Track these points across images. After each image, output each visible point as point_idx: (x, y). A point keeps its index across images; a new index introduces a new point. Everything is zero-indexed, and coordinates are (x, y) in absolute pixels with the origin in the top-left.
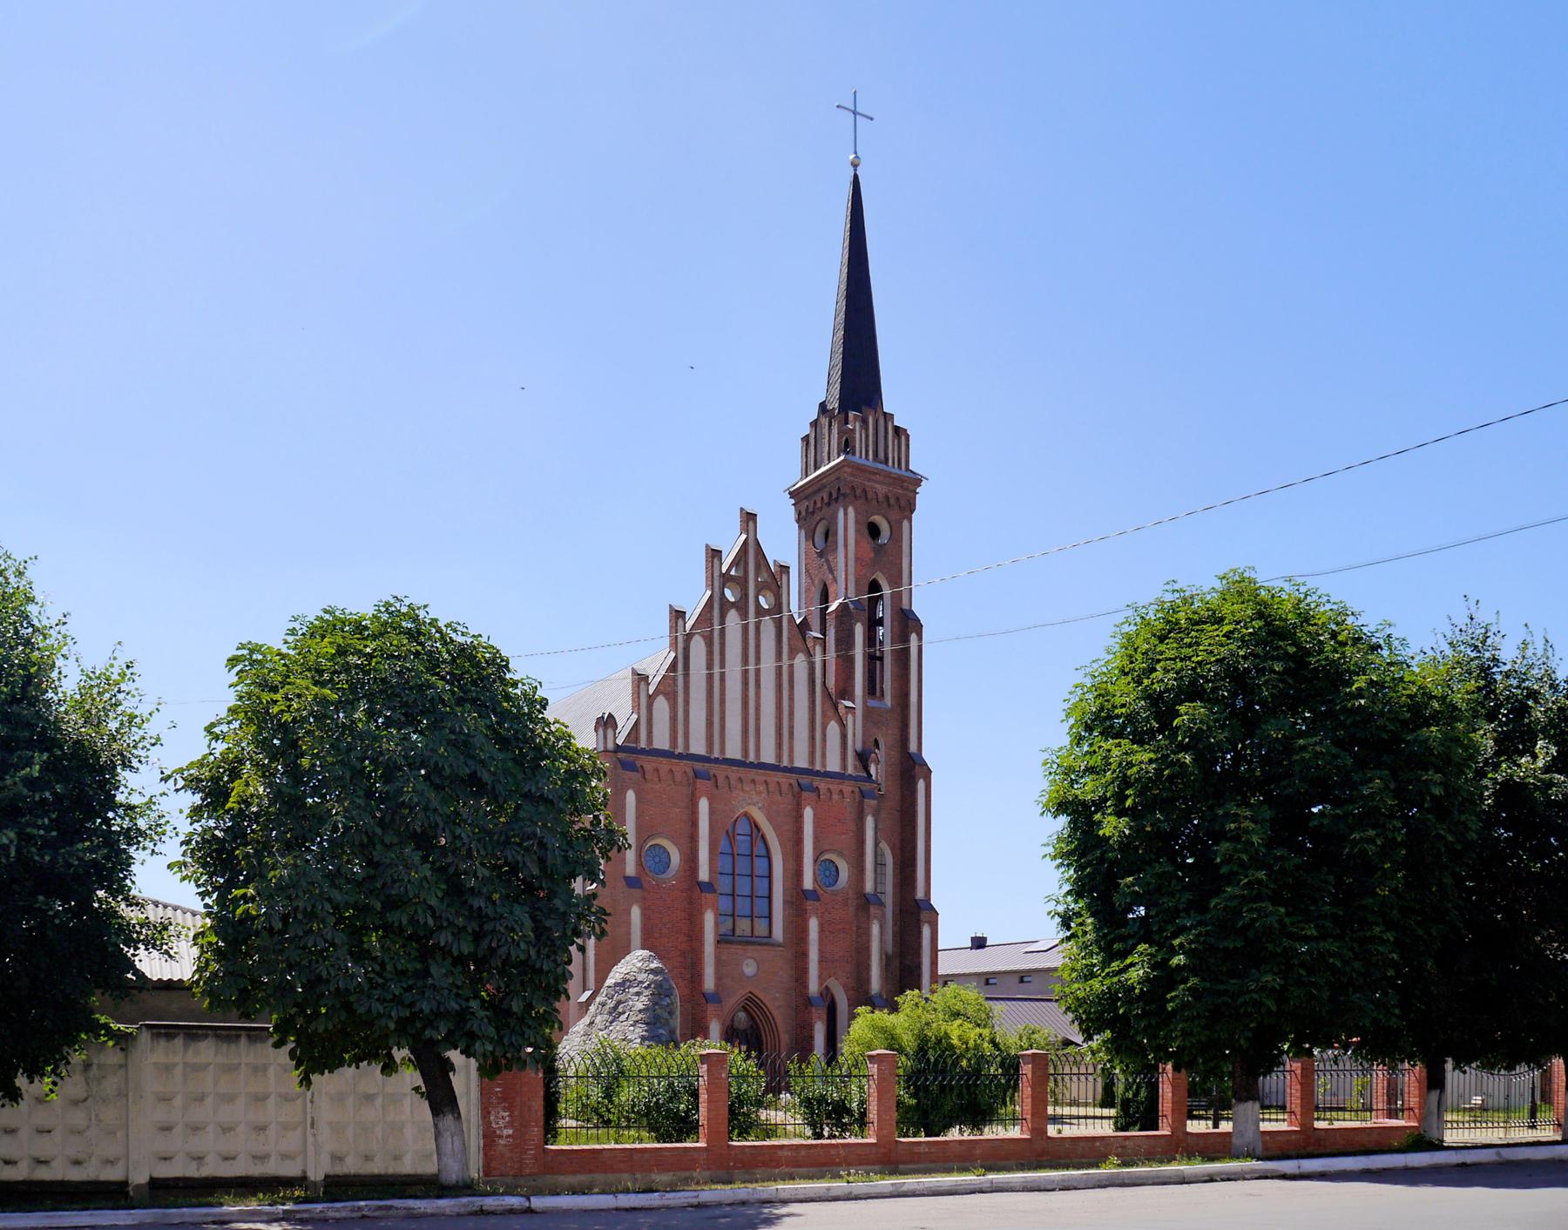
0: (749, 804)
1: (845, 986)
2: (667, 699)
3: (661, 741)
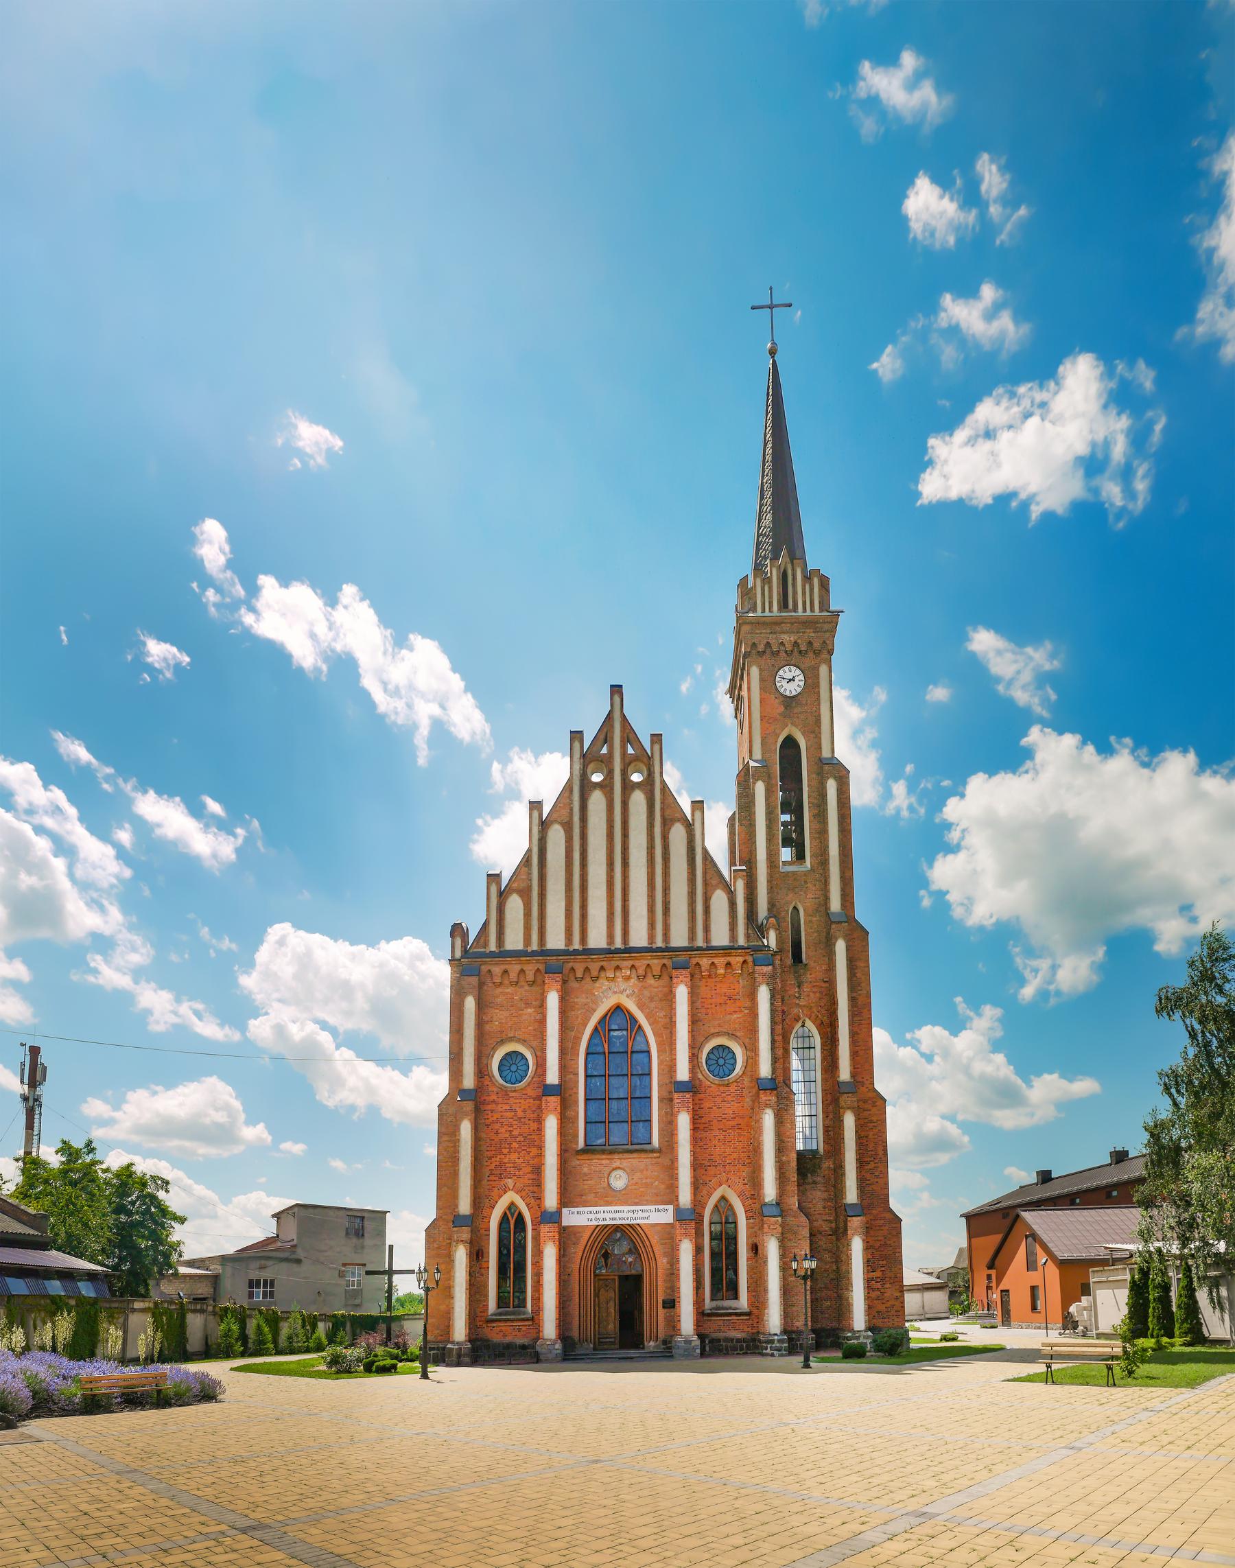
0: (615, 993)
2: (521, 896)
3: (514, 941)
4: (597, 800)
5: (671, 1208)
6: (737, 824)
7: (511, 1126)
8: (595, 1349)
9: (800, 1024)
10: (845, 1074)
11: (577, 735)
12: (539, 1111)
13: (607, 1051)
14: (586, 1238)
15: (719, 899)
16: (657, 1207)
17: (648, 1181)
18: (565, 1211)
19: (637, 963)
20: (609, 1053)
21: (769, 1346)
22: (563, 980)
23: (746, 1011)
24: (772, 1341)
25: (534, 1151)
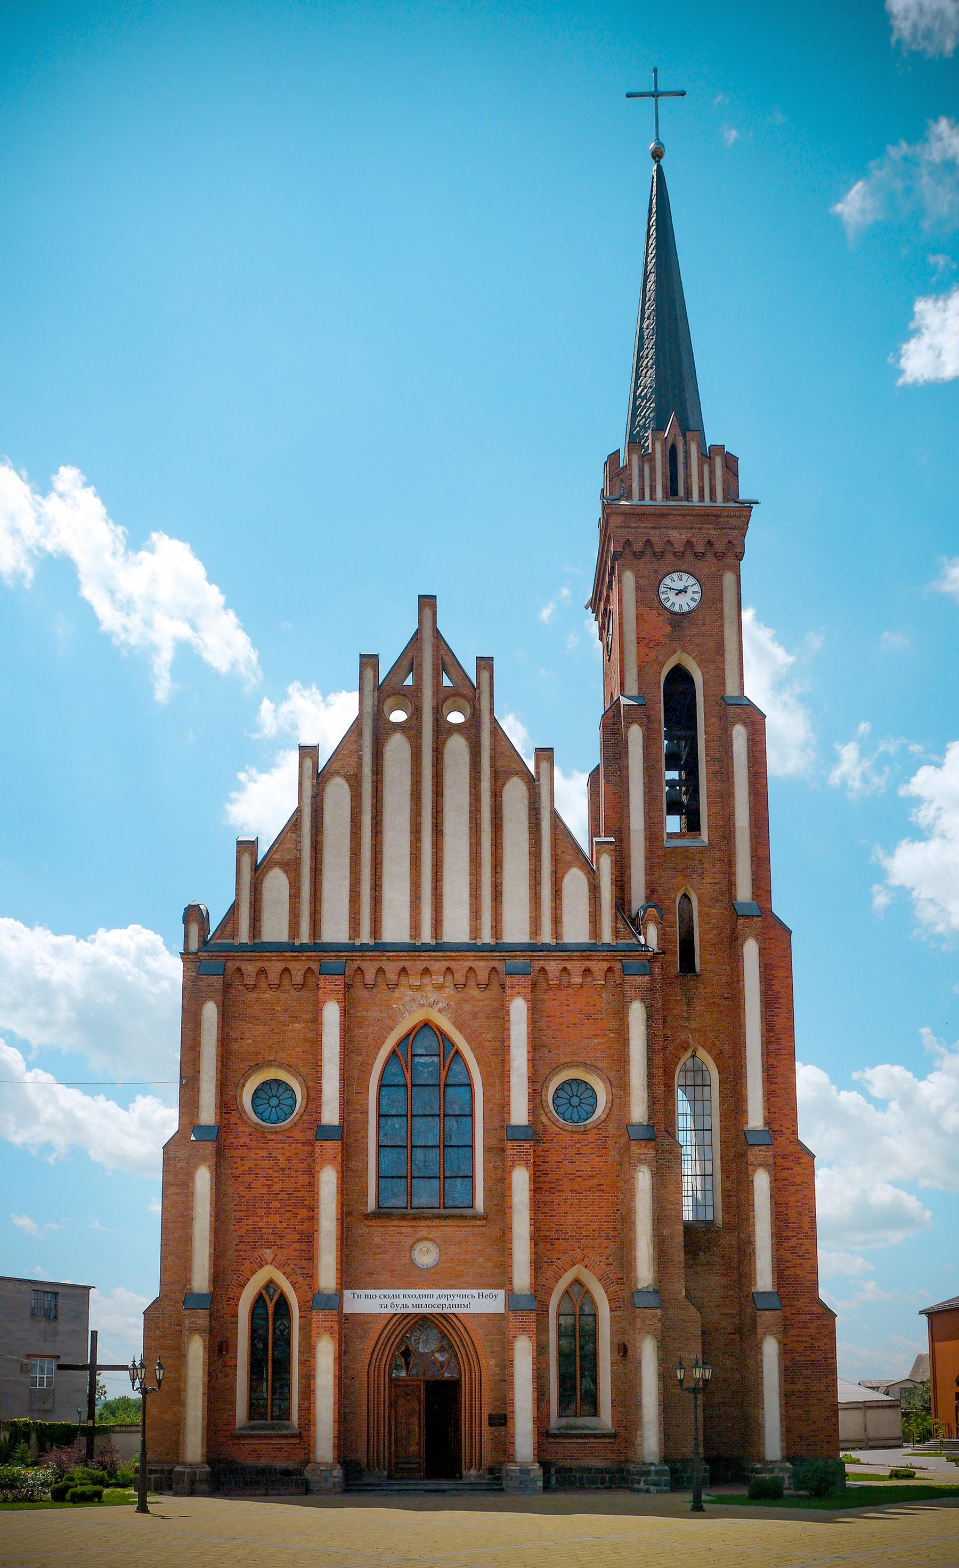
0: (423, 1005)
1: (602, 1279)
2: (286, 871)
5: (501, 1293)
6: (602, 781)
7: (269, 1178)
8: (389, 1477)
9: (689, 1053)
10: (755, 1118)
11: (369, 661)
12: (309, 1160)
13: (409, 1083)
15: (575, 881)
16: (481, 1291)
17: (469, 1256)
18: (348, 1293)
19: (454, 965)
20: (413, 1085)
21: (643, 1479)
22: (346, 984)
23: (612, 1035)
24: (647, 1473)
25: (303, 1213)
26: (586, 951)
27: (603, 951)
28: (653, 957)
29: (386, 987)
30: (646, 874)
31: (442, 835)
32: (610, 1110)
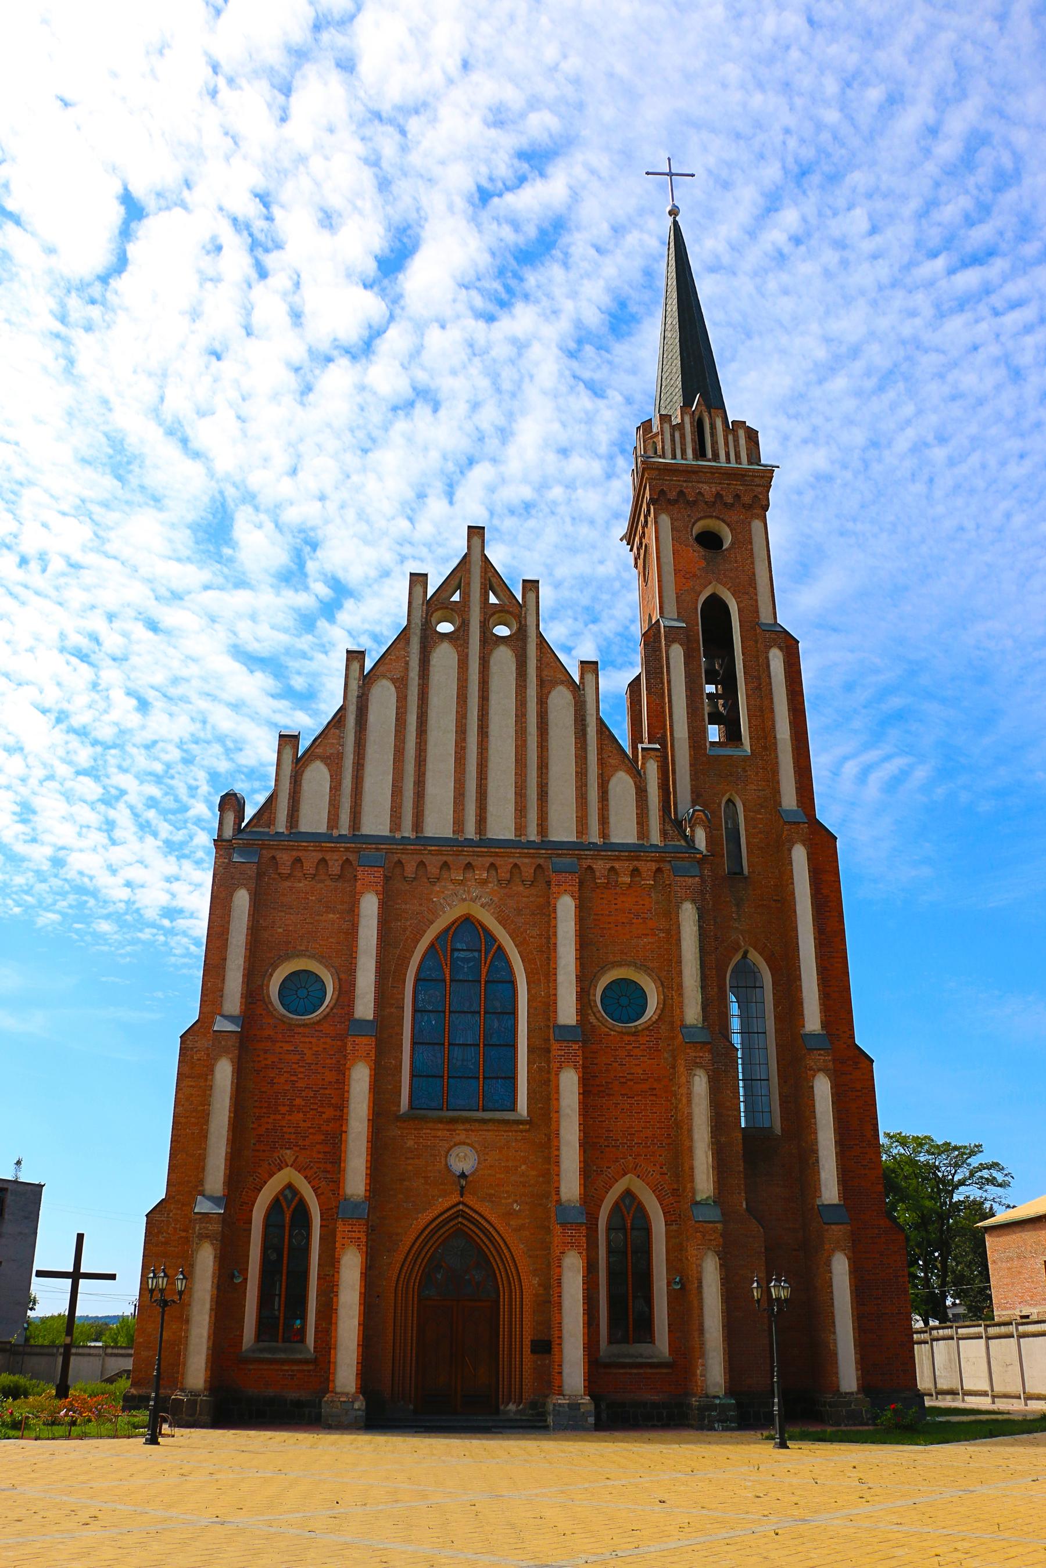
0: (464, 900)
1: (656, 1190)
2: (327, 765)
4: (444, 657)
10: (813, 1021)
14: (409, 1243)
15: (622, 784)
17: (510, 1164)
19: (498, 861)
20: (451, 981)
22: (385, 876)
23: (662, 935)
25: (329, 1113)
26: (633, 852)
27: (652, 852)
28: (702, 859)
29: (426, 880)
30: (692, 780)
31: (487, 737)
32: (662, 1011)
